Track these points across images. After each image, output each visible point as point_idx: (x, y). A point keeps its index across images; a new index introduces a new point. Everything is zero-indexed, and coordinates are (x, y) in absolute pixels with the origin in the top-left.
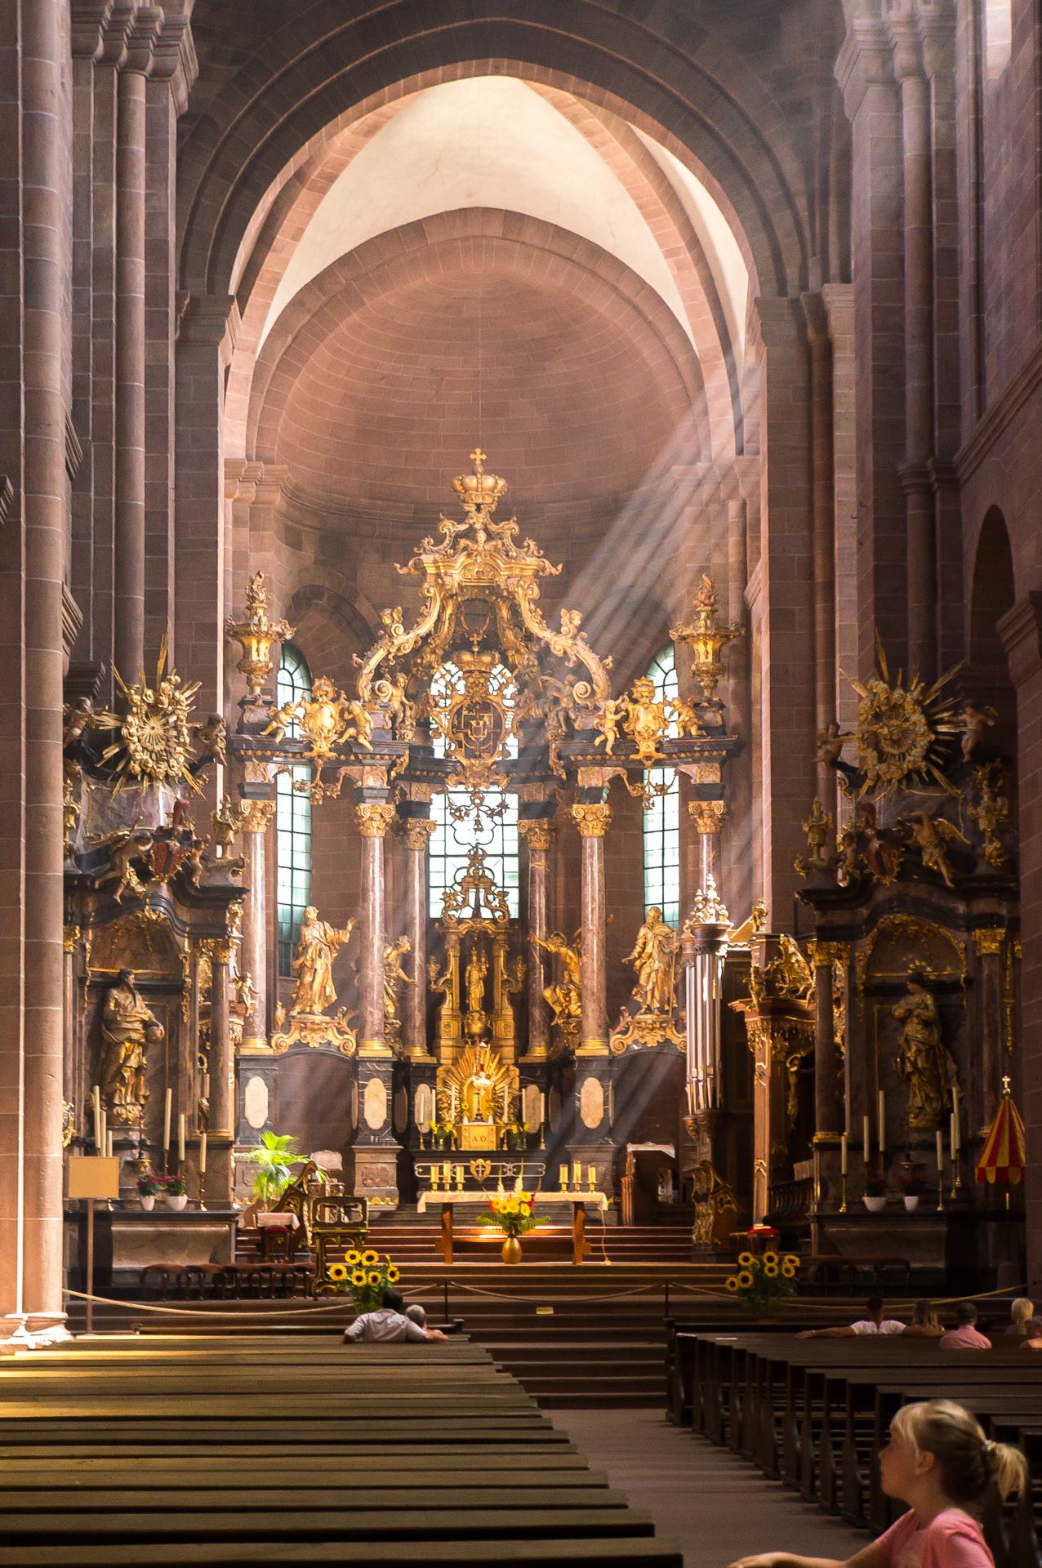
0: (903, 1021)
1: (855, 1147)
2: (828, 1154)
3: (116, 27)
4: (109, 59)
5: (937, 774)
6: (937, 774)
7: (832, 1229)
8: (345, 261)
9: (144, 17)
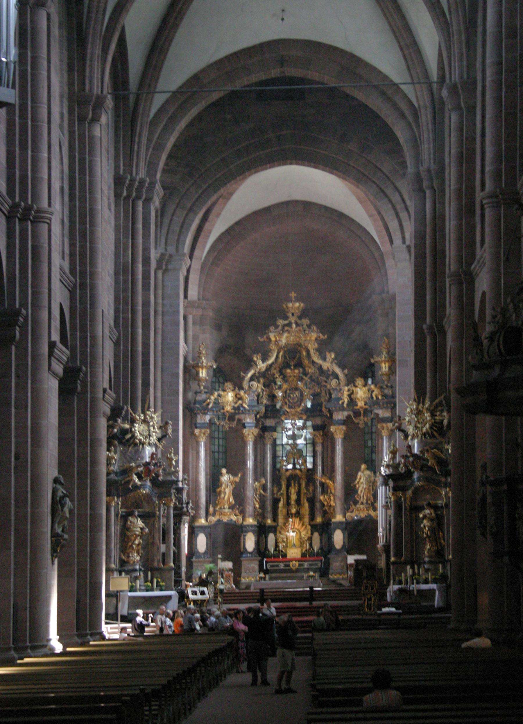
5: (435, 433)
6: (435, 433)
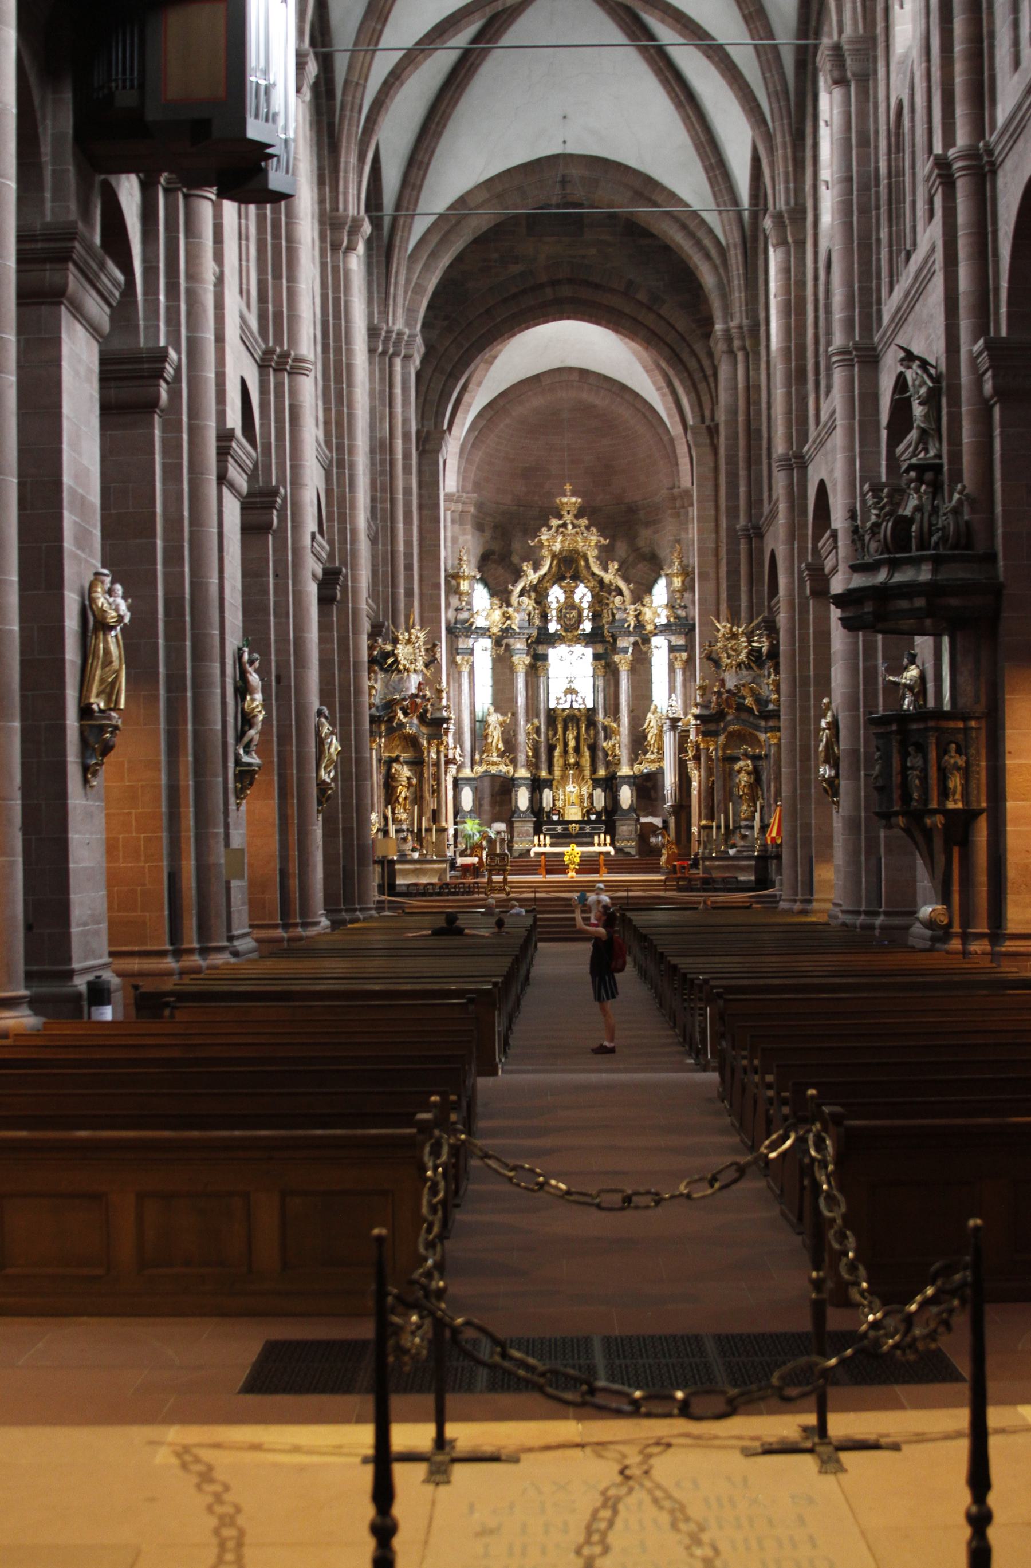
0: (739, 772)
1: (719, 827)
2: (706, 831)
3: (387, 339)
4: (384, 353)
7: (707, 863)
8: (503, 394)
9: (400, 334)
